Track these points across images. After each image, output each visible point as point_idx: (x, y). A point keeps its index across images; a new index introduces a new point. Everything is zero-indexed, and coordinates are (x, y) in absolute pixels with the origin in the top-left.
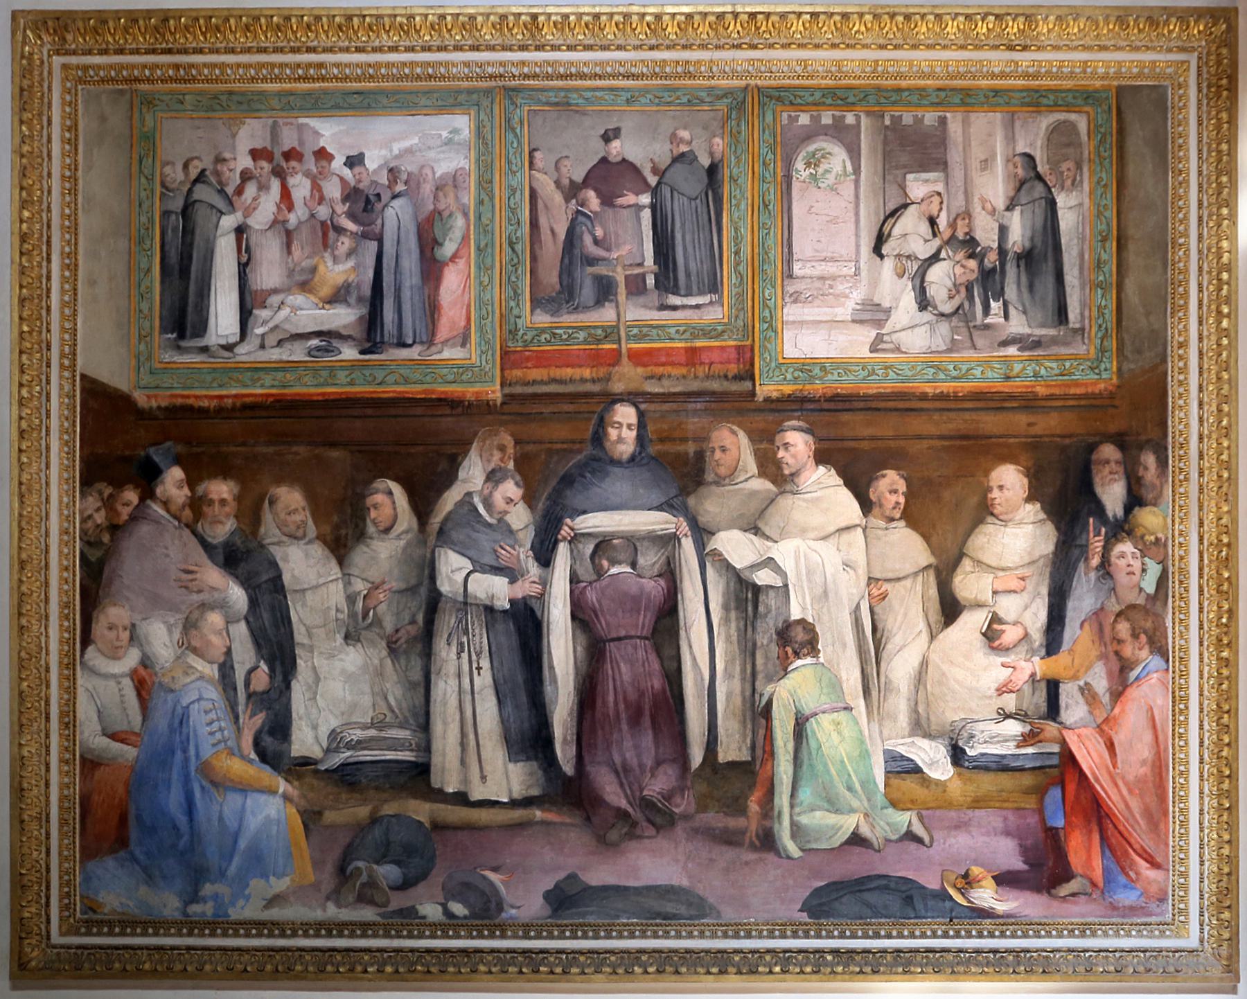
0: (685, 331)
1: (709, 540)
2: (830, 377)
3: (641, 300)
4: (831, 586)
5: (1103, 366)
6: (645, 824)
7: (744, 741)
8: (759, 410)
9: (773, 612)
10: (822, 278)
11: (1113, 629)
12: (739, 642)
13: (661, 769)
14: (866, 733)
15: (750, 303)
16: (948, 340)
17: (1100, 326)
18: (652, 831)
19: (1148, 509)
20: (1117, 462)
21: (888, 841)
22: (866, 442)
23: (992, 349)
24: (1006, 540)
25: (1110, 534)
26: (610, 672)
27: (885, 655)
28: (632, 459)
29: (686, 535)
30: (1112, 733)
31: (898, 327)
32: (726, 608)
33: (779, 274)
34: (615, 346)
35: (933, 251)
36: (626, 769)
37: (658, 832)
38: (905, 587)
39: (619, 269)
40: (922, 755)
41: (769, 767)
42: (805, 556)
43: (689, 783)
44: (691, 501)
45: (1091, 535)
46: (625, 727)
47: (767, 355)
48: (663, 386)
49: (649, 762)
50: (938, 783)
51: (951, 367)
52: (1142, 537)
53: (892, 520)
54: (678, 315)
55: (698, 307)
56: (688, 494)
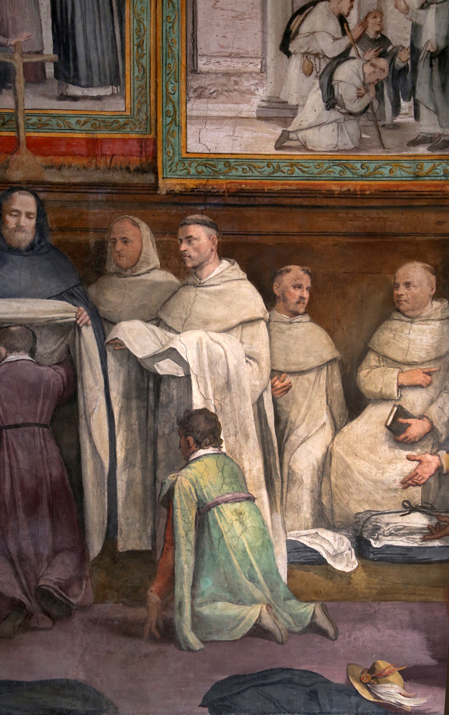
0: (85, 122)
1: (110, 330)
2: (234, 172)
3: (41, 88)
4: (233, 377)
6: (40, 615)
7: (145, 530)
8: (161, 203)
9: (175, 402)
10: (227, 74)
12: (140, 430)
13: (58, 559)
14: (269, 523)
15: (153, 96)
16: (355, 139)
18: (48, 623)
21: (291, 633)
22: (270, 238)
24: (412, 336)
26: (7, 459)
27: (288, 446)
28: (32, 247)
29: (86, 324)
31: (305, 124)
32: (126, 396)
33: (183, 69)
34: (13, 134)
35: (342, 49)
36: (22, 558)
37: (54, 624)
38: (308, 380)
39: (17, 56)
40: (326, 546)
41: (170, 557)
42: (208, 347)
43: (87, 573)
44: (92, 291)
46: (21, 515)
47: (170, 149)
48: (63, 176)
49: (46, 552)
50: (342, 574)
51: (358, 165)
53: (296, 314)
54: (79, 105)
55: (99, 98)
56: (89, 284)
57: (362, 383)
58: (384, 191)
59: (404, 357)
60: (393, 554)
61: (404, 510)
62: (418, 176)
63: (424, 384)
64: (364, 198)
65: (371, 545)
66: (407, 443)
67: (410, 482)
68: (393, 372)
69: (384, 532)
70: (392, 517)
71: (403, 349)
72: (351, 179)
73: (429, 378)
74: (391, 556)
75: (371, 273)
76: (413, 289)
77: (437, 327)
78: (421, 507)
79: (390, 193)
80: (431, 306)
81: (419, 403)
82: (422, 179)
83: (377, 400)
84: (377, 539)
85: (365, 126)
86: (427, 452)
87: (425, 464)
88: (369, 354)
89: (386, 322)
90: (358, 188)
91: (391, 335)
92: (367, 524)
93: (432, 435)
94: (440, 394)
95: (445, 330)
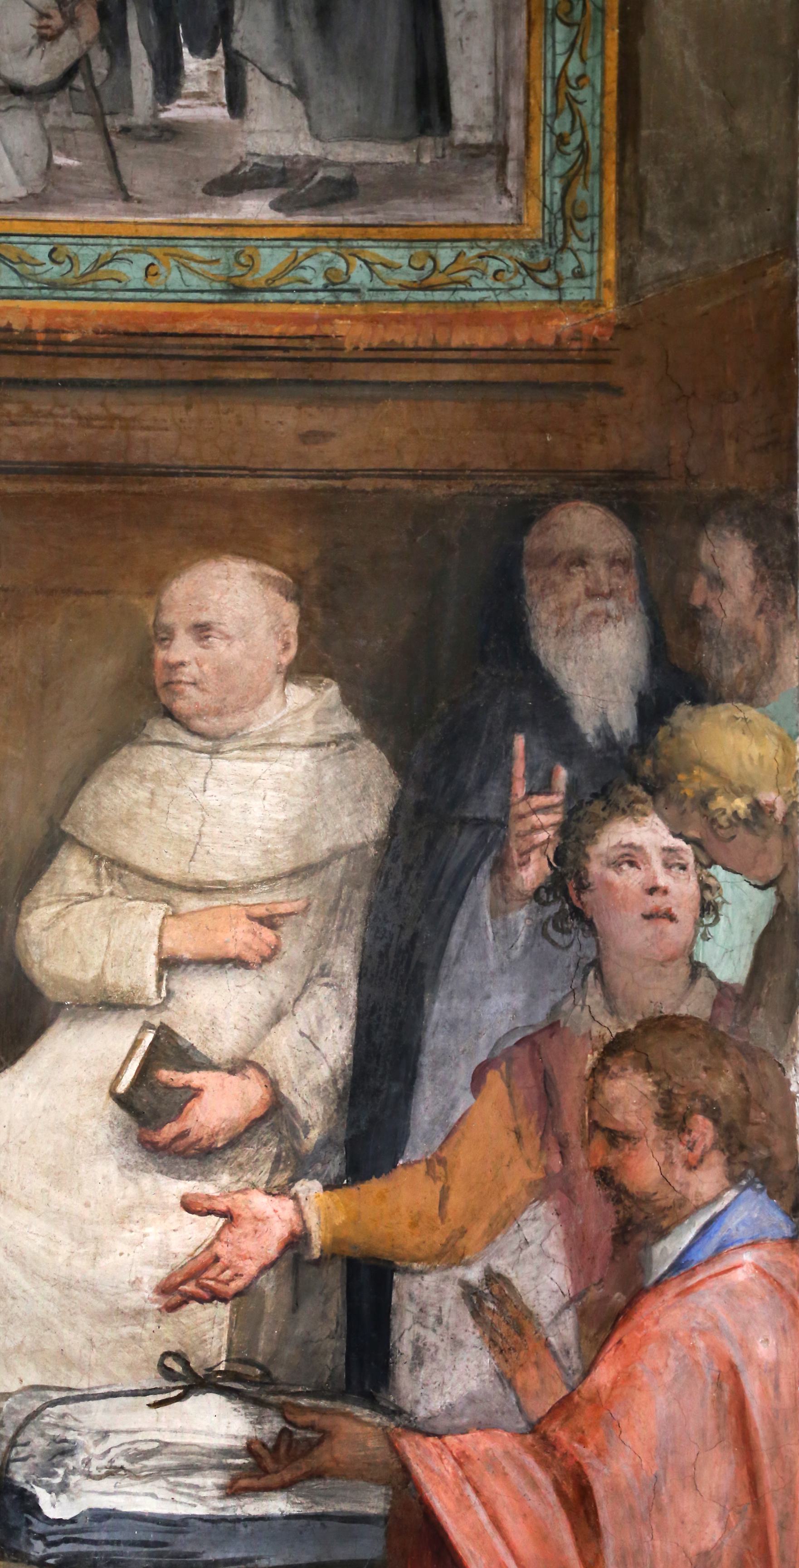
5: (568, 264)
11: (593, 1093)
16: (32, 169)
17: (562, 140)
19: (724, 711)
20: (612, 561)
23: (188, 202)
24: (214, 797)
25: (587, 790)
30: (585, 1453)
45: (520, 789)
51: (41, 252)
52: (704, 800)
57: (33, 949)
58: (127, 334)
59: (183, 866)
60: (118, 1543)
61: (165, 1384)
62: (240, 289)
63: (249, 956)
64: (60, 355)
65: (35, 1509)
66: (183, 1155)
67: (190, 1287)
68: (145, 915)
69: (87, 1462)
70: (119, 1411)
71: (182, 839)
72: (15, 292)
73: (268, 935)
74: (108, 1548)
75: (79, 592)
76: (219, 645)
77: (299, 769)
78: (227, 1374)
79: (147, 341)
80: (279, 701)
81: (231, 1020)
82: (252, 297)
83: (85, 1006)
84: (64, 1487)
85: (64, 129)
86: (254, 1186)
87: (248, 1228)
88: (63, 853)
89: (124, 751)
90: (38, 323)
91: (143, 795)
92: (30, 1433)
93: (276, 1130)
94: (305, 988)
95: (327, 779)
